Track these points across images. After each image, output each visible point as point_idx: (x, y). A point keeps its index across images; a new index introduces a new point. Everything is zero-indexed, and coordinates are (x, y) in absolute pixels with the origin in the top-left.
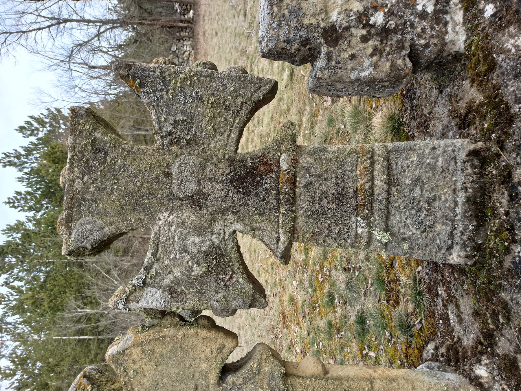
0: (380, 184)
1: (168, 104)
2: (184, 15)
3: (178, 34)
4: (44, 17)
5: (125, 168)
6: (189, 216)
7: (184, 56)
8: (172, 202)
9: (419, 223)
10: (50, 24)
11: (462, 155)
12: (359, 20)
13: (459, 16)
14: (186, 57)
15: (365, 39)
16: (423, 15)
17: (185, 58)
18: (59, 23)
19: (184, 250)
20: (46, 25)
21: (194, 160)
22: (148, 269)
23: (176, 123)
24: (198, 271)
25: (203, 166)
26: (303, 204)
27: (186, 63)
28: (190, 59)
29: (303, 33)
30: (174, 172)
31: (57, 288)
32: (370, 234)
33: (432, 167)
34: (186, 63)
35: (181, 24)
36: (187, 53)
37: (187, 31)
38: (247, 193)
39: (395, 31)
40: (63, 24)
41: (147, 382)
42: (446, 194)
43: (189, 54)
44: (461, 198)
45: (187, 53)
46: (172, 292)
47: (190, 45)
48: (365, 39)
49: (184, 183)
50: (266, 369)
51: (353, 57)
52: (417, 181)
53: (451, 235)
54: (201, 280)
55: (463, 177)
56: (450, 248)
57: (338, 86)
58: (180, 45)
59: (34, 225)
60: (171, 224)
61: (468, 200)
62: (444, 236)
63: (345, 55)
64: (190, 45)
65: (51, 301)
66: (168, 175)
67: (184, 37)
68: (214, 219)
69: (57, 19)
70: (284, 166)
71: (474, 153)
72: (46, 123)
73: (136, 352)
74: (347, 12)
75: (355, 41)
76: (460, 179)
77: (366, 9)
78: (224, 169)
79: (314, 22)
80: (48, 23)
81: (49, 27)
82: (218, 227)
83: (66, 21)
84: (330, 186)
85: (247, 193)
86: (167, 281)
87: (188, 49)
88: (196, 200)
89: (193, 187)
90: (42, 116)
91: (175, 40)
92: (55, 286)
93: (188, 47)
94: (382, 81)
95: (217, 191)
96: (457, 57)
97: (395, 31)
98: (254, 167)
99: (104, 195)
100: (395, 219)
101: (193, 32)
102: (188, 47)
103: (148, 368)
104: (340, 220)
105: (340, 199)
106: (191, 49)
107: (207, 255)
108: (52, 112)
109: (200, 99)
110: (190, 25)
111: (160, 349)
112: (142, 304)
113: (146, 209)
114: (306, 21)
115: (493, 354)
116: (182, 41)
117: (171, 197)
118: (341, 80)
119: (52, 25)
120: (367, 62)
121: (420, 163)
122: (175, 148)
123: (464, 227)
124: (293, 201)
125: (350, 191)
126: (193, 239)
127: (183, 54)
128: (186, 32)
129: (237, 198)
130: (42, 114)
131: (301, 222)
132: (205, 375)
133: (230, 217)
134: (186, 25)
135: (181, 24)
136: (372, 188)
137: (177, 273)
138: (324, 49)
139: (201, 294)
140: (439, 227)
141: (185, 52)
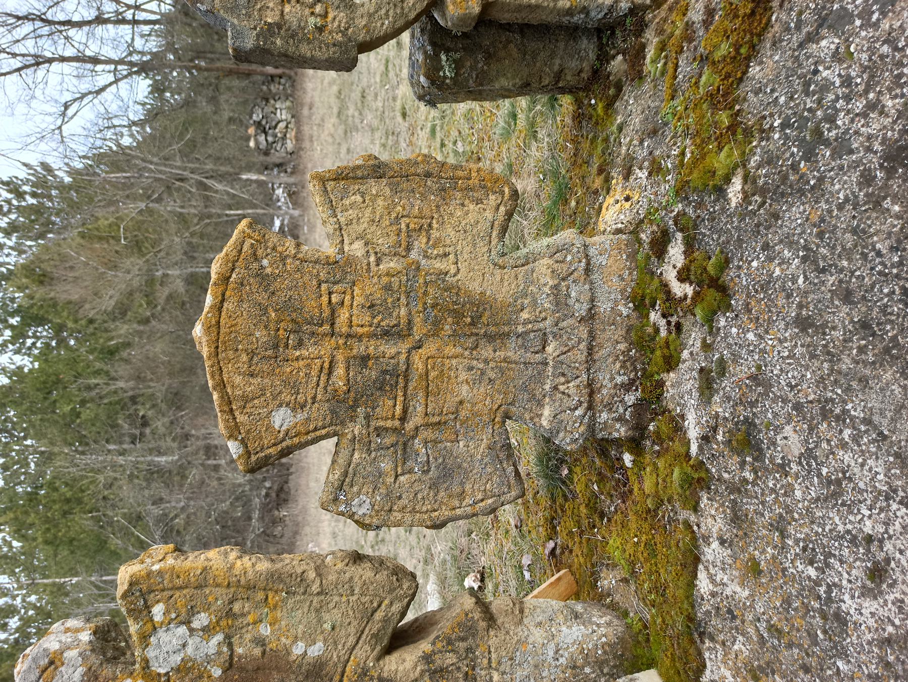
3: (265, 88)
4: (8, 53)
7: (277, 130)
10: (19, 65)
14: (281, 132)
17: (279, 135)
18: (38, 64)
20: (15, 67)
27: (280, 145)
28: (288, 136)
31: (57, 507)
34: (280, 145)
36: (282, 125)
37: (283, 81)
40: (47, 65)
43: (287, 127)
45: (282, 125)
47: (288, 108)
58: (268, 109)
59: (10, 378)
64: (288, 108)
65: (48, 530)
67: (275, 94)
69: (32, 56)
72: (25, 193)
80: (16, 63)
81: (18, 70)
83: (50, 61)
87: (284, 117)
90: (14, 180)
91: (259, 101)
92: (54, 501)
93: (284, 112)
101: (293, 86)
102: (284, 112)
106: (289, 116)
108: (35, 170)
116: (272, 102)
119: (26, 67)
127: (275, 127)
128: (279, 83)
130: (16, 178)
141: (279, 122)
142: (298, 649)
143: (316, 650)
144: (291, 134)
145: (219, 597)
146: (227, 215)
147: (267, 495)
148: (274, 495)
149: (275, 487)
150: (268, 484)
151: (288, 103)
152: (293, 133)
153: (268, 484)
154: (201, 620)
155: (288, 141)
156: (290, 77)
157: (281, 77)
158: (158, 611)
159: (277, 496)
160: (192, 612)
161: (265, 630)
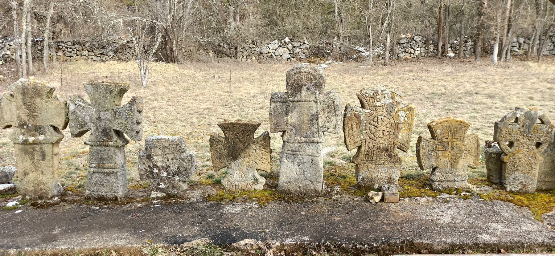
0: (106, 170)
2: (451, 47)
3: (431, 42)
5: (106, 99)
6: (95, 117)
9: (96, 182)
11: (116, 194)
12: (155, 165)
13: (159, 195)
15: (149, 167)
16: (158, 184)
17: (407, 49)
21: (110, 118)
24: (80, 119)
25: (109, 120)
26: (100, 148)
27: (402, 50)
29: (149, 149)
30: (107, 112)
33: (112, 186)
34: (402, 50)
35: (441, 44)
36: (412, 51)
39: (153, 175)
41: (50, 106)
43: (411, 53)
44: (104, 194)
45: (412, 51)
46: (74, 112)
48: (149, 167)
49: (103, 115)
50: (54, 138)
51: (144, 163)
52: (108, 181)
54: (77, 120)
55: (110, 194)
56: (90, 190)
58: (420, 44)
62: (93, 189)
63: (144, 161)
66: (105, 111)
67: (428, 47)
68: (94, 123)
70: (110, 143)
71: (116, 198)
73: (58, 102)
74: (157, 161)
75: (149, 164)
77: (159, 167)
79: (153, 152)
82: (92, 124)
84: (105, 156)
86: (77, 111)
87: (416, 52)
88: (99, 118)
89: (102, 118)
93: (419, 52)
95: (102, 124)
97: (153, 175)
98: (109, 135)
99: (99, 93)
100: (97, 175)
103: (54, 106)
104: (96, 159)
105: (102, 159)
107: (84, 122)
110: (440, 53)
111: (59, 109)
113: (96, 105)
114: (152, 149)
115: (60, 202)
116: (424, 46)
117: (100, 112)
120: (143, 167)
121: (113, 182)
123: (95, 194)
125: (104, 162)
127: (411, 48)
129: (100, 130)
131: (95, 148)
132: (52, 121)
133: (95, 128)
134: (440, 49)
135: (441, 44)
137: (79, 113)
139: (73, 120)
140: (96, 187)
142: (400, 134)
143: (400, 137)
144: (408, 56)
145: (409, 122)
146: (369, 27)
147: (221, 46)
148: (221, 49)
149: (224, 50)
150: (226, 46)
151: (423, 54)
152: (408, 57)
153: (226, 46)
154: (406, 119)
155: (404, 54)
156: (437, 55)
157: (437, 50)
158: (408, 112)
159: (220, 51)
160: (408, 118)
161: (404, 129)
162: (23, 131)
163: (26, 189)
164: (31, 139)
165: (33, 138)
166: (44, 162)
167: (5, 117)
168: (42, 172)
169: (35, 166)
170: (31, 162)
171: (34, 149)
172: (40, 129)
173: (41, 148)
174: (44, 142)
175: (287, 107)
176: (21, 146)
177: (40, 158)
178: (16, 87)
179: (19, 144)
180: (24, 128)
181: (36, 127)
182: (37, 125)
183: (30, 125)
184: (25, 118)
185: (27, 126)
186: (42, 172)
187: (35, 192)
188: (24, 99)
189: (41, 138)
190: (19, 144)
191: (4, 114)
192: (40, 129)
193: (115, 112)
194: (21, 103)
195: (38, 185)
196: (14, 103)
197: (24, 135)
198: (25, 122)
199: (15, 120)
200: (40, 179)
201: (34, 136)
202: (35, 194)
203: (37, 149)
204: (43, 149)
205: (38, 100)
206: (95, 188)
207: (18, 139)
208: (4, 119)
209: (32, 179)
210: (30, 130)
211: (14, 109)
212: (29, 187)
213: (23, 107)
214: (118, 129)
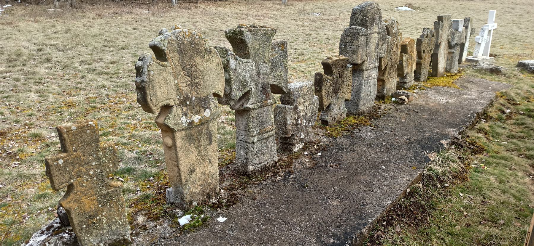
1: (280, 60)
6: (255, 72)
8: (258, 65)
19: (246, 72)
22: (240, 60)
23: (276, 63)
24: (241, 78)
26: (260, 111)
30: (265, 65)
32: (254, 136)
38: (261, 91)
42: (265, 158)
44: (266, 163)
46: (235, 70)
53: (256, 164)
56: (252, 165)
57: (283, 114)
60: (252, 66)
61: (265, 166)
66: (264, 63)
76: (270, 161)
78: (266, 82)
82: (253, 83)
85: (261, 91)
86: (238, 68)
88: (258, 74)
89: (262, 72)
94: (286, 128)
95: (261, 81)
96: (291, 151)
107: (245, 81)
109: (282, 70)
112: (231, 60)
117: (259, 65)
118: (285, 114)
122: (270, 64)
124: (261, 107)
126: (248, 75)
136: (266, 132)
137: (240, 71)
138: (292, 107)
162: (185, 109)
163: (192, 192)
164: (197, 118)
165: (199, 117)
166: (211, 146)
167: (158, 94)
168: (210, 160)
169: (202, 155)
170: (197, 152)
171: (200, 132)
172: (204, 101)
173: (208, 128)
174: (211, 118)
175: (367, 40)
176: (183, 132)
177: (207, 142)
178: (169, 43)
179: (183, 130)
180: (186, 105)
181: (200, 99)
182: (202, 96)
183: (194, 98)
184: (186, 89)
185: (190, 100)
186: (210, 160)
187: (202, 193)
188: (181, 61)
189: (207, 113)
190: (183, 130)
191: (157, 88)
192: (204, 101)
193: (272, 63)
194: (179, 67)
195: (205, 180)
196: (169, 69)
197: (186, 115)
198: (187, 95)
199: (174, 96)
200: (208, 171)
201: (198, 113)
202: (203, 194)
203: (203, 130)
204: (210, 129)
205: (198, 60)
206: (256, 161)
207: (182, 123)
208: (157, 96)
209: (199, 175)
210: (194, 106)
211: (171, 78)
212: (196, 188)
213: (182, 73)
214: (274, 83)
